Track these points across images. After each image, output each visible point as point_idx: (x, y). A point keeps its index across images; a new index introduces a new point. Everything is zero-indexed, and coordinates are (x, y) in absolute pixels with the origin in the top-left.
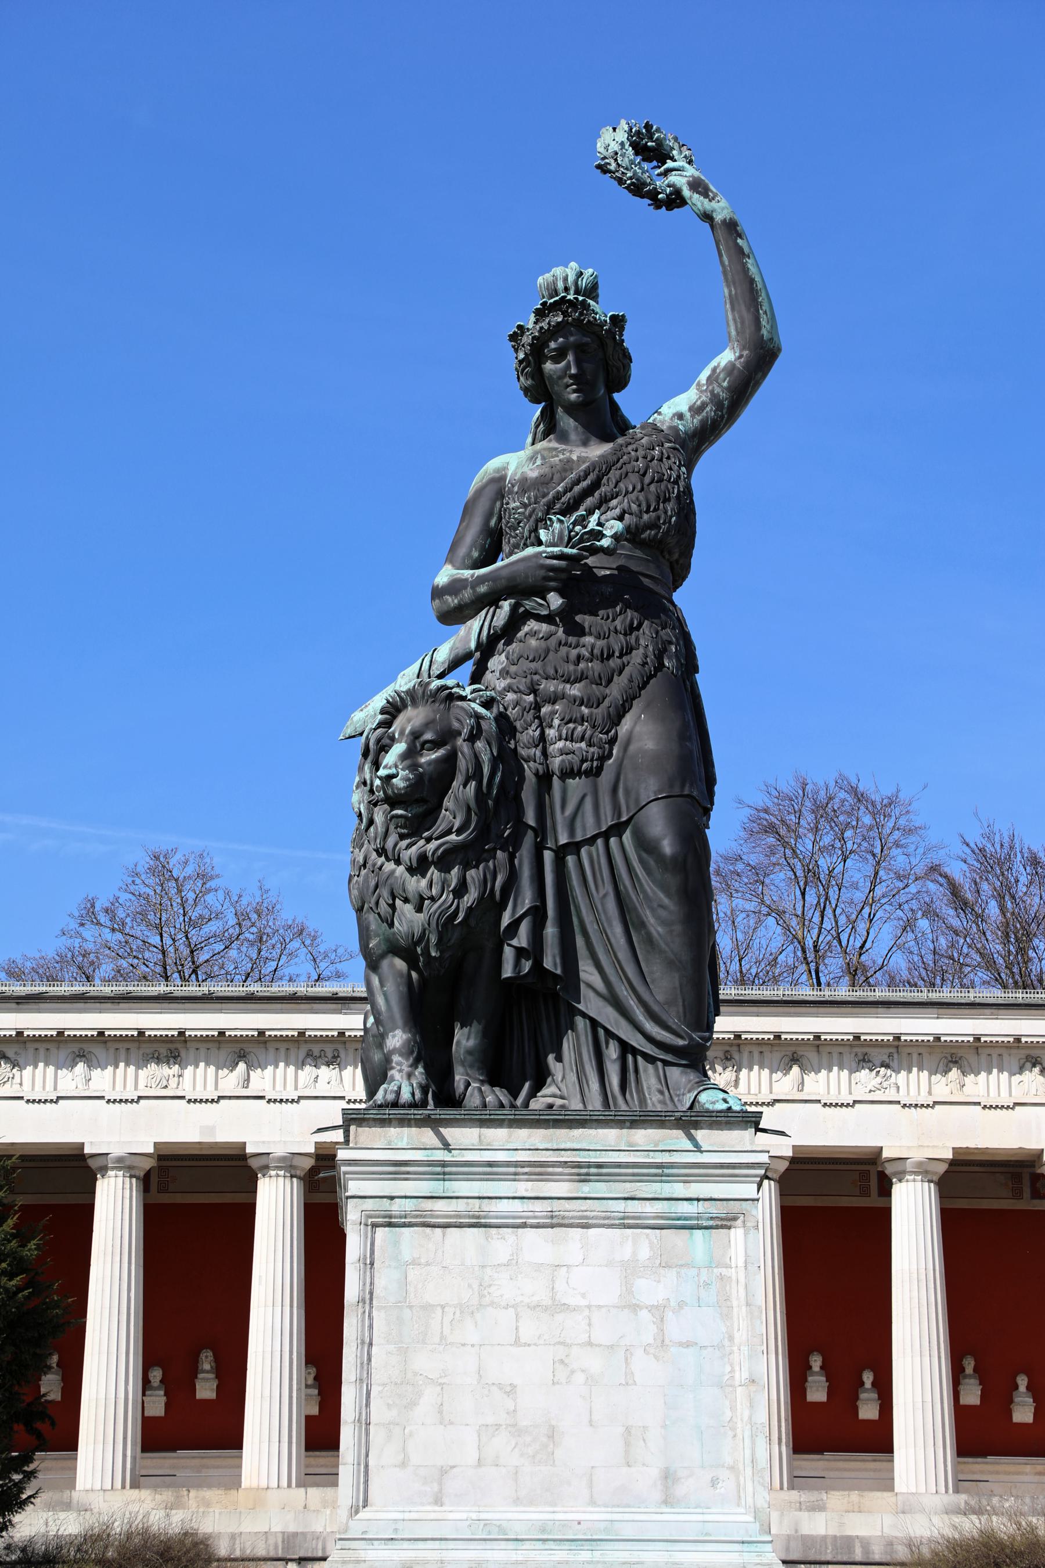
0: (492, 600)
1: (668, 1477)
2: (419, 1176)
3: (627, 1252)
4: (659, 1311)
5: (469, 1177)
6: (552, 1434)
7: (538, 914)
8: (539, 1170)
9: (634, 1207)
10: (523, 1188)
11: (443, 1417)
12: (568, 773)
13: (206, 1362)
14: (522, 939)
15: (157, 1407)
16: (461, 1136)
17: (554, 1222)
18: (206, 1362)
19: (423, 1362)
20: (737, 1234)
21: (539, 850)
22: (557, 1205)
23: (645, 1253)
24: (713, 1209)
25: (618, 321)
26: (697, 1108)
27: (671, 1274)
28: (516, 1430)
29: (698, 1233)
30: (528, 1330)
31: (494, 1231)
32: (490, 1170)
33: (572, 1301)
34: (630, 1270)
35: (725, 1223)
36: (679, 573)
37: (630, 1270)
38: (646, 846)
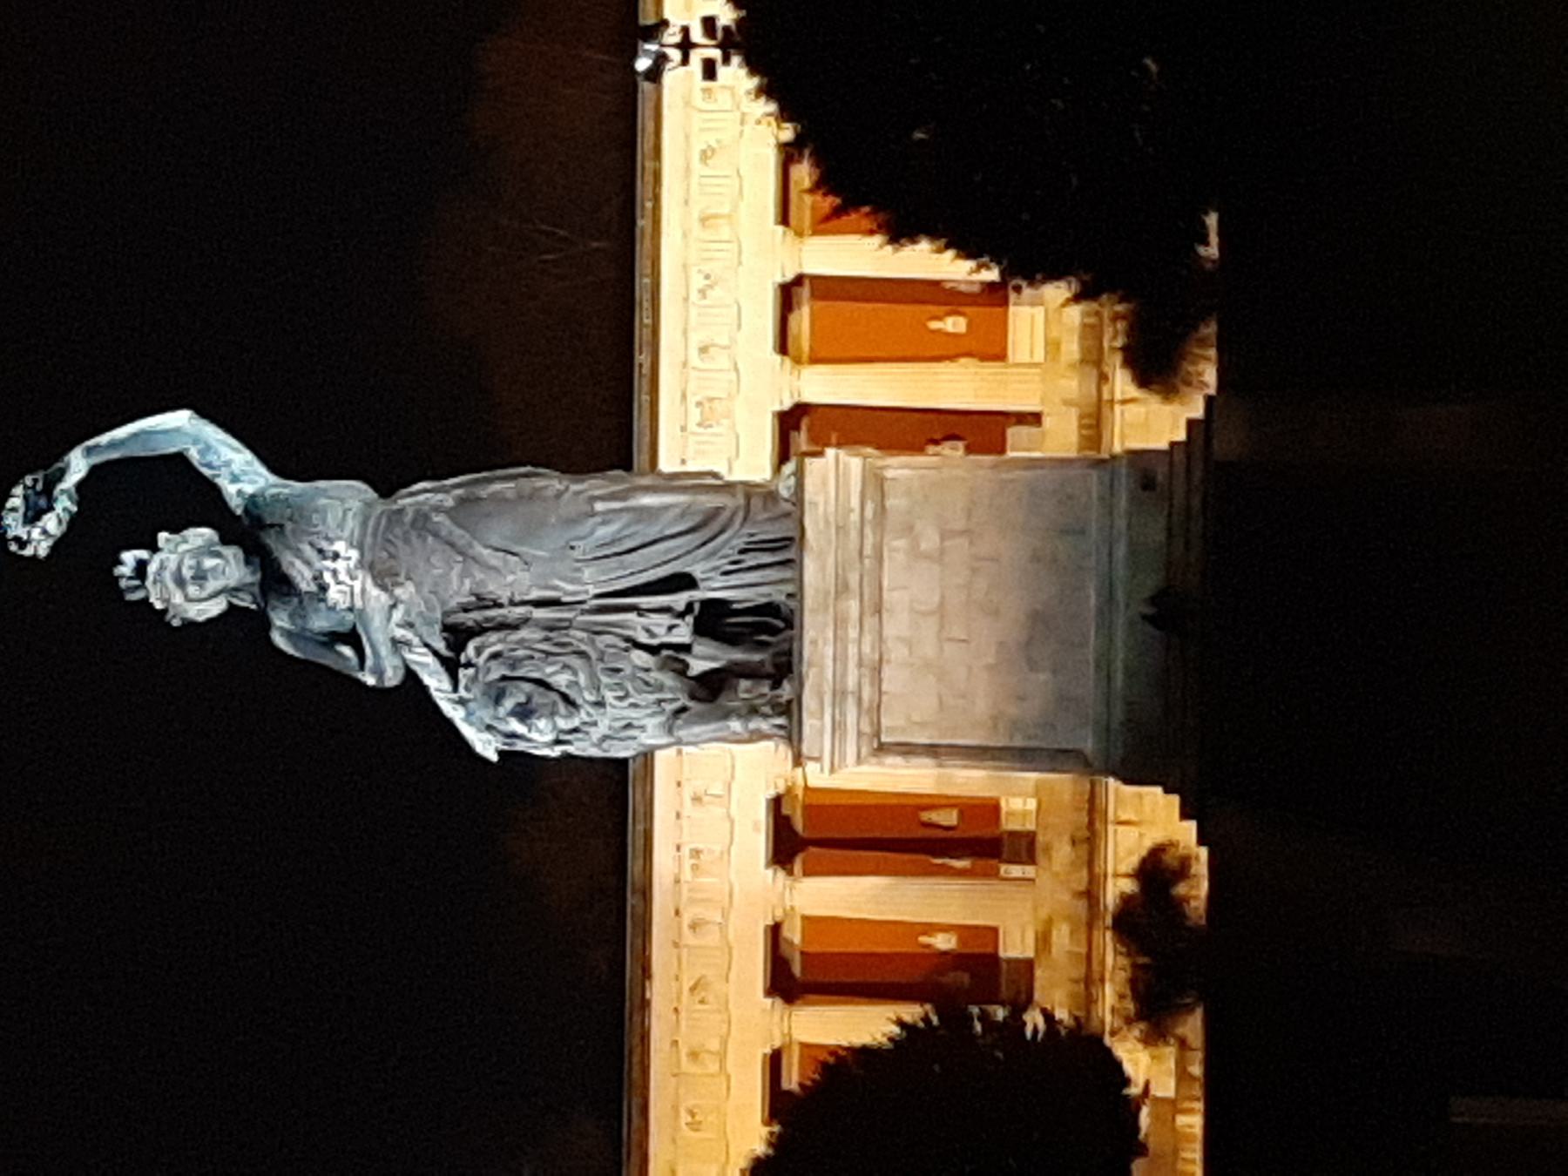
2: (843, 714)
3: (900, 557)
5: (844, 674)
8: (840, 623)
9: (868, 550)
10: (853, 633)
17: (878, 610)
20: (889, 474)
22: (866, 609)
23: (901, 543)
24: (870, 491)
26: (794, 499)
27: (919, 526)
29: (889, 503)
31: (885, 657)
32: (839, 658)
33: (937, 599)
35: (880, 482)
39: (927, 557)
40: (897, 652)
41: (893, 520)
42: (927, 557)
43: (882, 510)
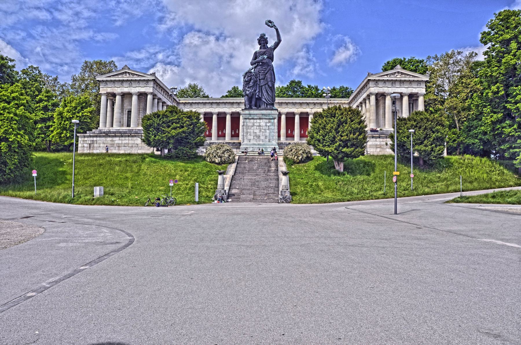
0: (255, 64)
1: (269, 140)
4: (269, 126)
6: (259, 136)
7: (259, 92)
11: (250, 135)
12: (262, 79)
13: (237, 130)
14: (258, 94)
15: (233, 133)
16: (252, 112)
17: (260, 119)
18: (237, 130)
19: (249, 131)
21: (259, 86)
25: (267, 38)
28: (256, 136)
30: (257, 128)
32: (254, 114)
34: (266, 123)
35: (274, 119)
36: (272, 61)
37: (266, 123)
38: (268, 86)
39: (266, 124)
40: (255, 121)
41: (270, 120)
42: (266, 124)
43: (271, 119)
